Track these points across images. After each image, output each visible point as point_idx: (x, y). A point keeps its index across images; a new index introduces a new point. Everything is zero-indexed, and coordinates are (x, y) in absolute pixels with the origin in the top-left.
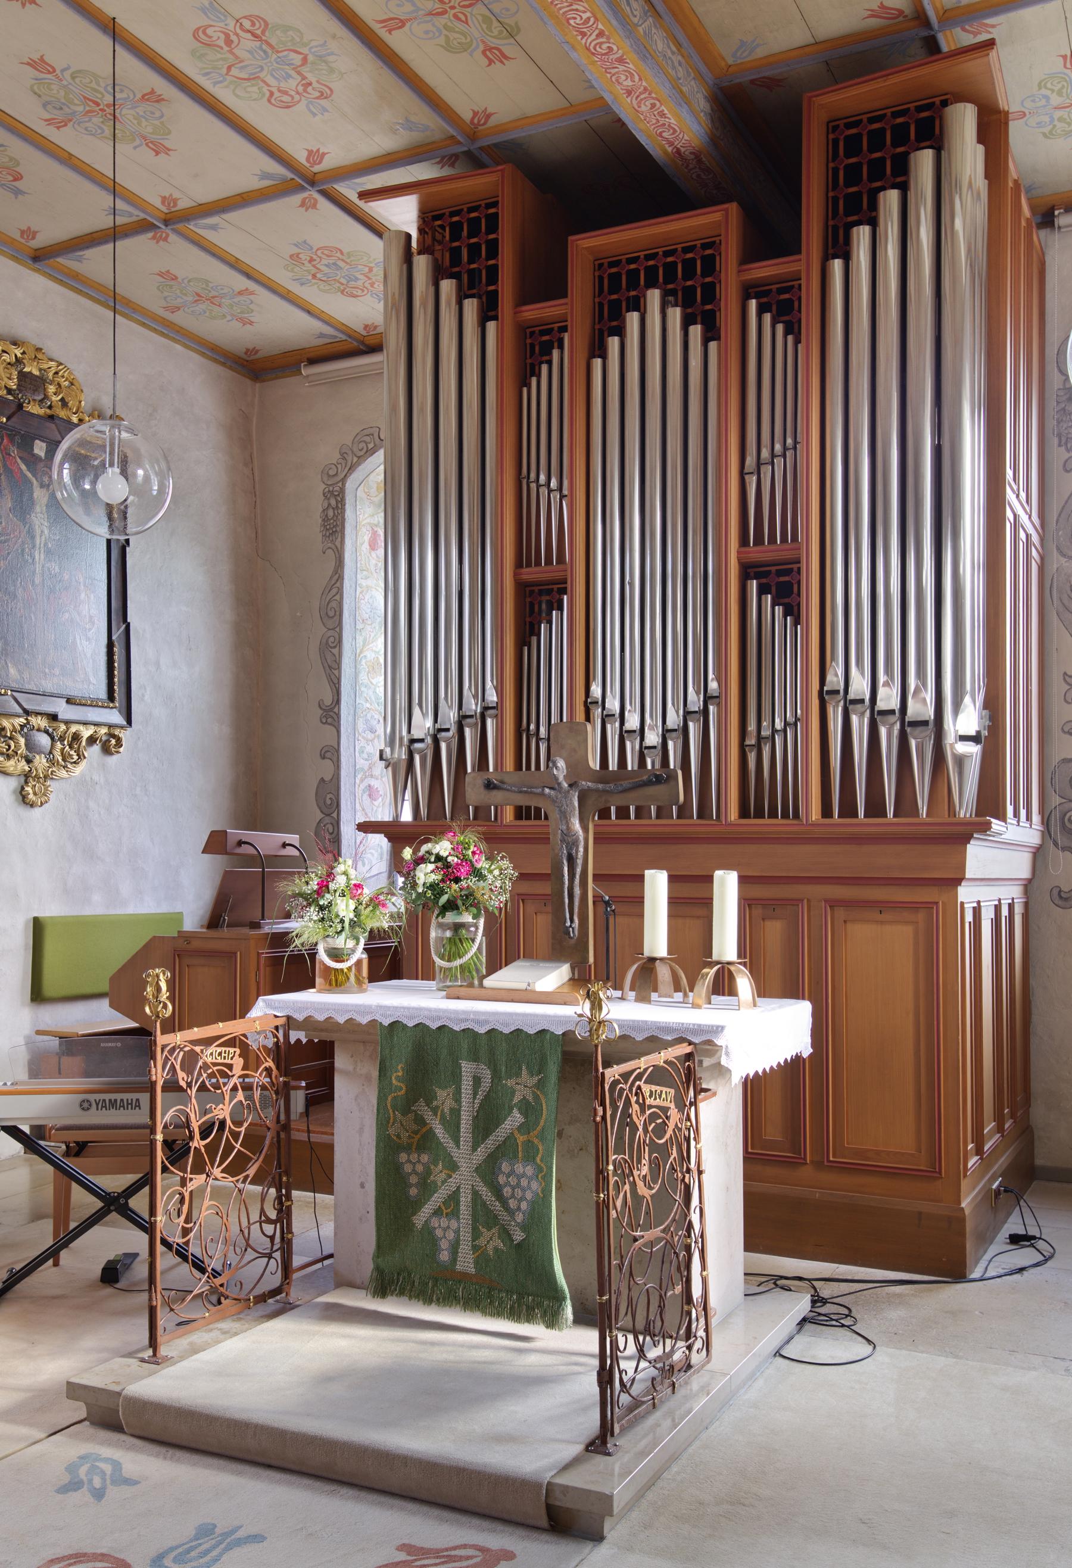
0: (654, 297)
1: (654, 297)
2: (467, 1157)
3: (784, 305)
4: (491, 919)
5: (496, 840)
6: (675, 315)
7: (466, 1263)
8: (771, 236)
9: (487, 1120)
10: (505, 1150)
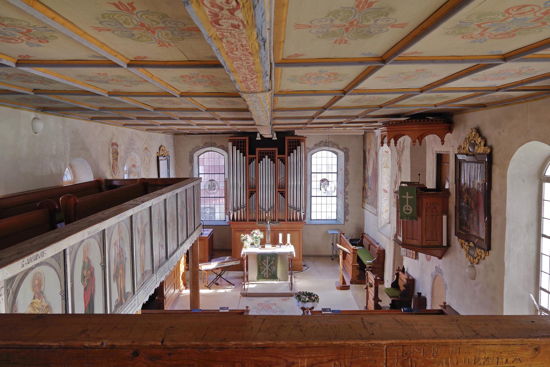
0: (267, 157)
1: (267, 157)
2: (267, 266)
3: (283, 161)
4: (261, 239)
5: (261, 231)
6: (269, 159)
7: (267, 277)
8: (282, 152)
9: (269, 262)
10: (272, 265)
